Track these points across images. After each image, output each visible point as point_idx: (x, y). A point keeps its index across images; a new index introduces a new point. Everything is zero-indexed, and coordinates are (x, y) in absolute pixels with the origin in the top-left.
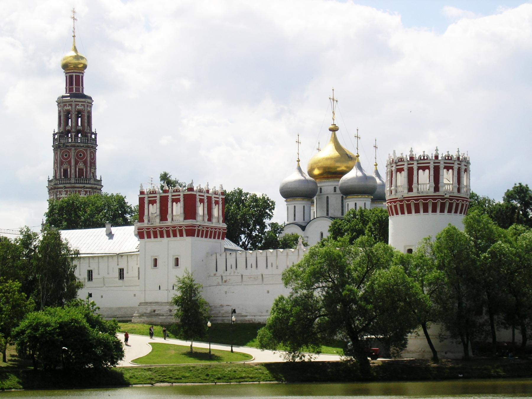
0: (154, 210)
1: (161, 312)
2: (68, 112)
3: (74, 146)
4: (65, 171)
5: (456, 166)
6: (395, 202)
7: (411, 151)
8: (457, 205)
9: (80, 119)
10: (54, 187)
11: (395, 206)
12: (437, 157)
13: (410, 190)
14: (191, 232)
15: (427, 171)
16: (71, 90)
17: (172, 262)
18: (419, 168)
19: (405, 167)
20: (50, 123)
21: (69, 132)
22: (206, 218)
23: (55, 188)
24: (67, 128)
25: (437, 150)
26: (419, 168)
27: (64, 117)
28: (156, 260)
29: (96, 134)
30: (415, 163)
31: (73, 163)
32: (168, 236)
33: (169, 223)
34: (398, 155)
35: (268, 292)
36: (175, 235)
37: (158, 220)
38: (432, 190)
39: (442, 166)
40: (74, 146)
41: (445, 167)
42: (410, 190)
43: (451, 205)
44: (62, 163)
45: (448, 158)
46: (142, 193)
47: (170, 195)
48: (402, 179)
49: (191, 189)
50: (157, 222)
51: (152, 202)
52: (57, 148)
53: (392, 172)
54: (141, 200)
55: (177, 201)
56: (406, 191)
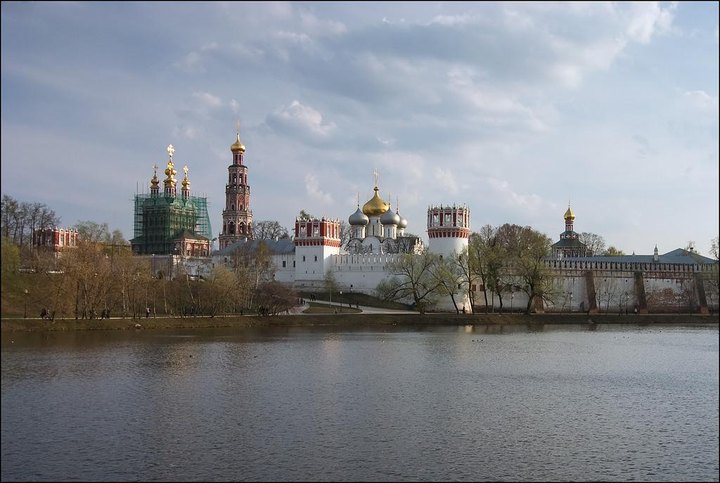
0: (304, 230)
1: (308, 285)
4: (233, 206)
10: (226, 215)
12: (454, 208)
13: (441, 225)
18: (446, 214)
19: (439, 213)
20: (225, 180)
21: (235, 185)
26: (446, 214)
27: (233, 176)
28: (304, 257)
36: (315, 245)
37: (306, 236)
39: (457, 213)
42: (441, 225)
46: (297, 221)
48: (437, 219)
49: (323, 220)
51: (303, 226)
52: (228, 193)
54: (297, 225)
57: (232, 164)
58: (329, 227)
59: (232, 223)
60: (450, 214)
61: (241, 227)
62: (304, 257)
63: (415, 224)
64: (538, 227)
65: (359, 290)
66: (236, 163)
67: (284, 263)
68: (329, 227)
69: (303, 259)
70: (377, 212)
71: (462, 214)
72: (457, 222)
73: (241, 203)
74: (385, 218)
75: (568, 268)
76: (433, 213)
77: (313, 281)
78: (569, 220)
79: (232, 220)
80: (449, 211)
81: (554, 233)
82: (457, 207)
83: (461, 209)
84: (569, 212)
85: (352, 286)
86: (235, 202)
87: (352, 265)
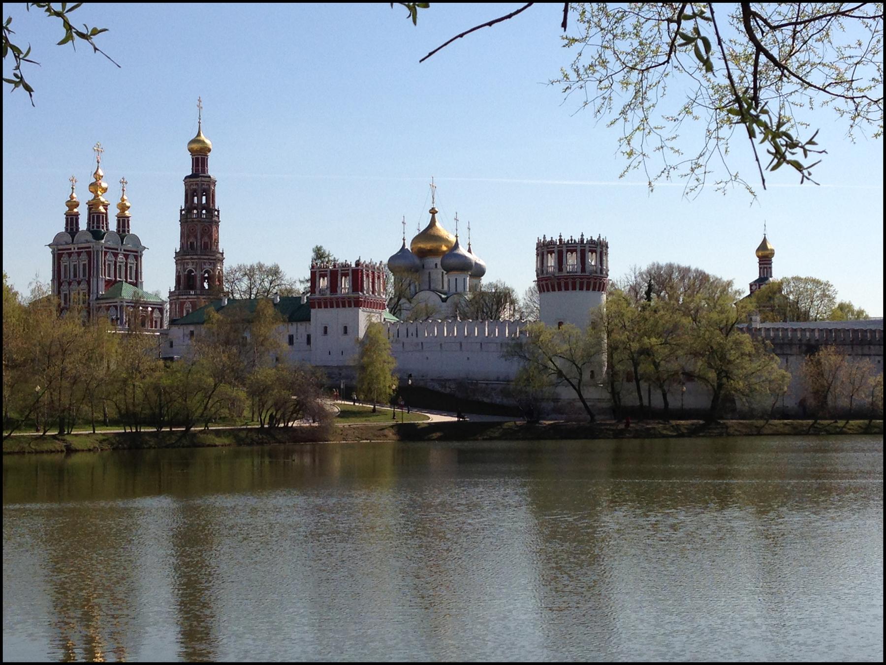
2: (195, 191)
3: (200, 221)
4: (192, 244)
5: (599, 250)
8: (600, 284)
9: (204, 198)
10: (180, 257)
11: (547, 284)
13: (560, 269)
14: (358, 304)
16: (197, 170)
17: (341, 330)
19: (556, 250)
25: (582, 235)
27: (190, 195)
28: (326, 328)
29: (218, 211)
31: (199, 237)
34: (548, 239)
36: (344, 306)
37: (328, 292)
38: (579, 270)
39: (587, 249)
40: (200, 221)
41: (590, 251)
42: (560, 269)
43: (595, 284)
44: (188, 237)
45: (592, 241)
46: (313, 267)
48: (551, 261)
51: (323, 276)
54: (313, 274)
55: (346, 275)
57: (190, 173)
58: (368, 276)
59: (191, 271)
61: (206, 278)
63: (511, 269)
64: (716, 270)
66: (197, 170)
68: (368, 276)
73: (206, 239)
76: (544, 248)
79: (190, 267)
81: (741, 276)
85: (410, 376)
86: (196, 238)
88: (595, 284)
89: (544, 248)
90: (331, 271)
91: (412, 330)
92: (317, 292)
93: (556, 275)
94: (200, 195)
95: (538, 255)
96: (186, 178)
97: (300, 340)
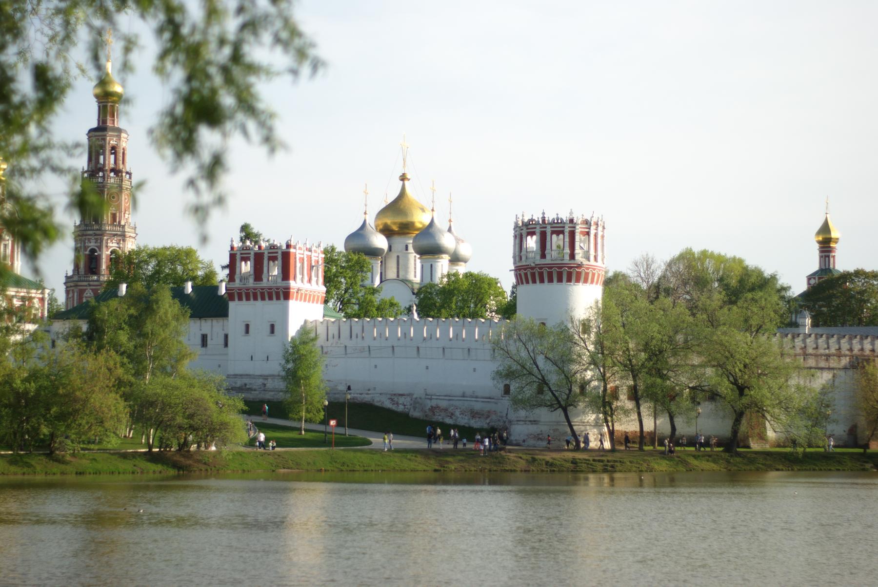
0: (246, 268)
6: (525, 269)
7: (544, 213)
8: (594, 275)
9: (112, 157)
11: (526, 274)
12: (571, 221)
13: (543, 256)
15: (561, 236)
17: (268, 329)
19: (538, 230)
22: (306, 278)
23: (83, 235)
24: (99, 166)
25: (571, 213)
26: (553, 232)
28: (247, 326)
30: (549, 227)
32: (263, 299)
33: (264, 283)
35: (376, 366)
36: (271, 298)
37: (251, 280)
38: (567, 257)
41: (581, 233)
42: (543, 256)
46: (232, 248)
47: (266, 252)
48: (532, 243)
49: (288, 246)
50: (251, 283)
51: (245, 259)
53: (521, 235)
54: (232, 257)
55: (273, 259)
56: (538, 257)
57: (95, 125)
59: (93, 251)
60: (562, 232)
62: (247, 326)
65: (367, 398)
66: (104, 122)
67: (204, 338)
68: (302, 260)
69: (243, 328)
70: (406, 228)
71: (588, 234)
72: (578, 250)
74: (425, 243)
75: (821, 351)
76: (524, 229)
77: (265, 377)
78: (826, 245)
79: (92, 245)
80: (558, 227)
82: (578, 218)
83: (587, 223)
84: (825, 228)
85: (349, 388)
87: (349, 344)
88: (587, 274)
89: (524, 229)
90: (256, 254)
91: (357, 329)
92: (237, 281)
93: (538, 262)
94: (107, 153)
95: (515, 237)
96: (91, 131)
97: (215, 341)
